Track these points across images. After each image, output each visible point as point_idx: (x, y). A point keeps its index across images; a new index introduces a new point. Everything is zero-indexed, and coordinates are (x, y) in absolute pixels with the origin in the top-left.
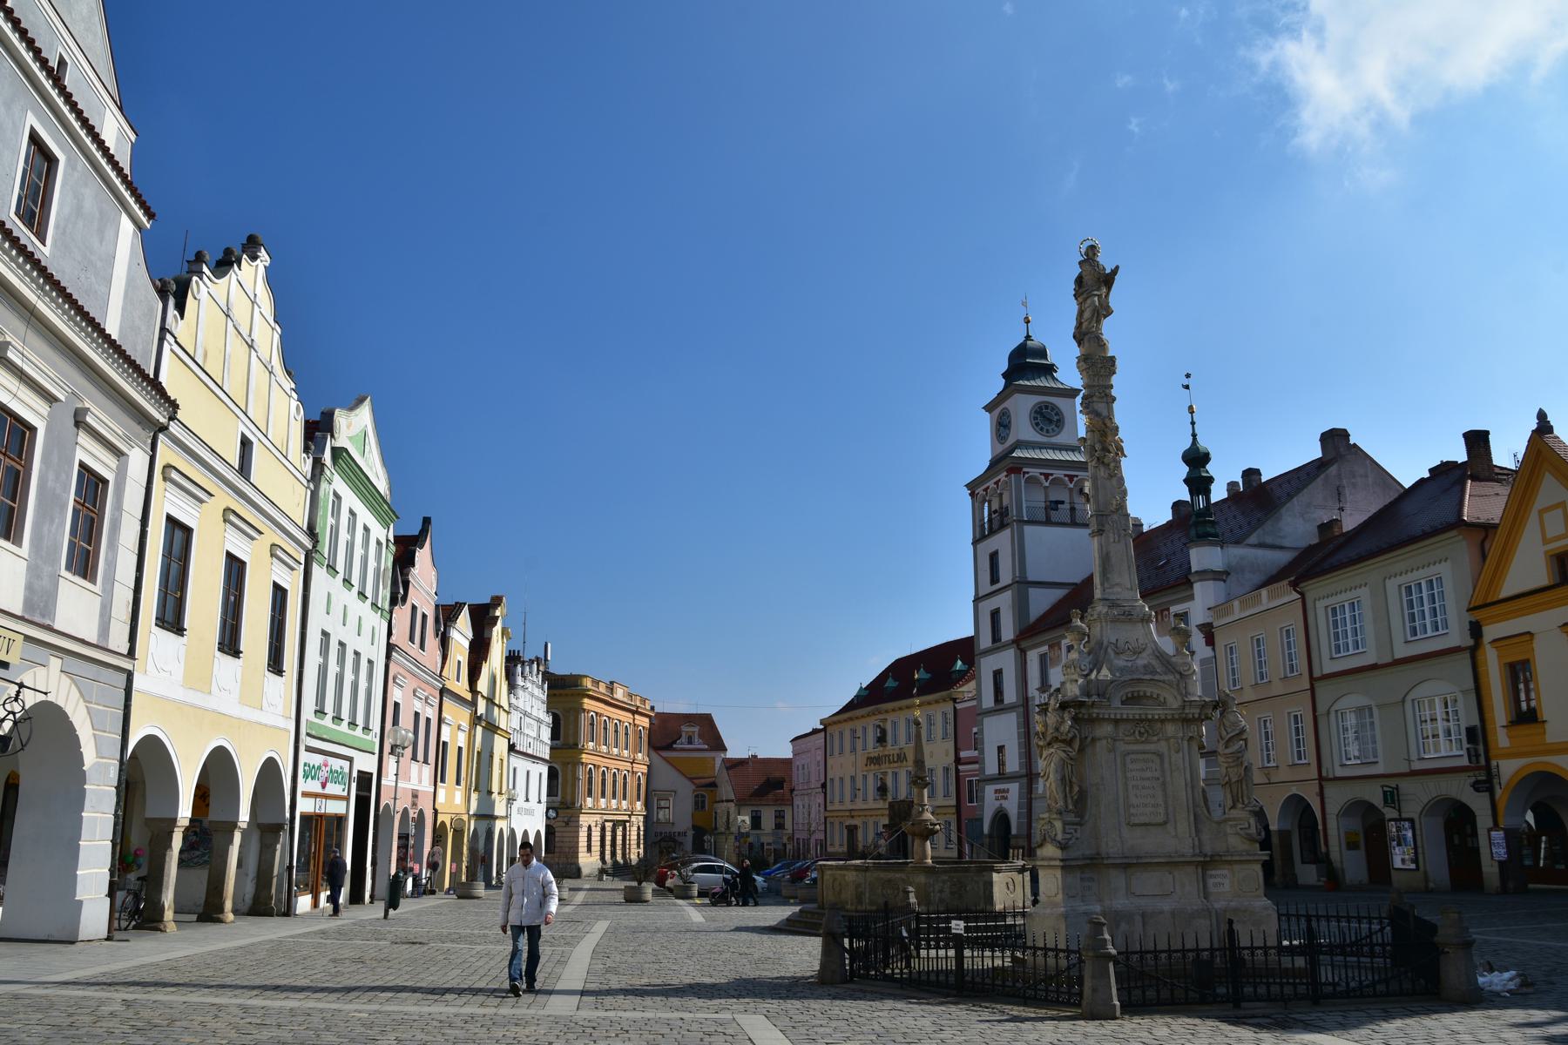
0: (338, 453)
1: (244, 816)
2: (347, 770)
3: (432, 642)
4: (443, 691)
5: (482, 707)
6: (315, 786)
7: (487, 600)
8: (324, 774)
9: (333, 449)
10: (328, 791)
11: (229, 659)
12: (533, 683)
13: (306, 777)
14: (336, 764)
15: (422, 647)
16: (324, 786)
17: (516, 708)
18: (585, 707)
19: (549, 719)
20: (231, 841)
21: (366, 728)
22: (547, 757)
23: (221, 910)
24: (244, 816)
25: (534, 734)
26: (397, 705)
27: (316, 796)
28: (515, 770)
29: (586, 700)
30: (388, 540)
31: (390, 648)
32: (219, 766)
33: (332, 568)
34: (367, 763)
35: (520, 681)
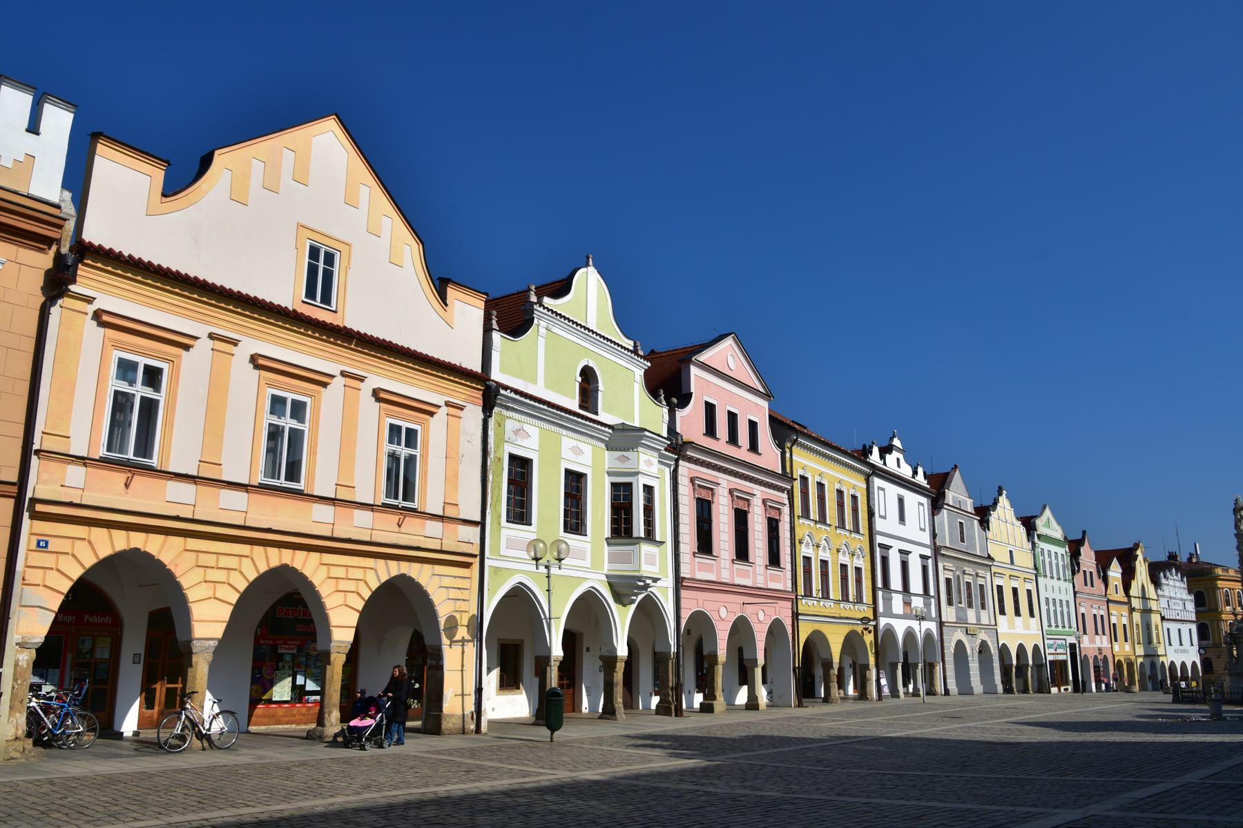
0: (1039, 536)
1: (1031, 662)
2: (1064, 643)
3: (1098, 583)
4: (1108, 601)
5: (1136, 603)
6: (1052, 651)
7: (1132, 546)
8: (1055, 646)
9: (1038, 535)
10: (1058, 651)
11: (1018, 617)
12: (1174, 580)
13: (1048, 648)
14: (1059, 642)
15: (1092, 586)
16: (1056, 650)
17: (1164, 596)
18: (1219, 586)
19: (1192, 597)
20: (1028, 670)
21: (1070, 627)
22: (1194, 619)
23: (1029, 690)
24: (1031, 662)
25: (1181, 608)
26: (1083, 614)
27: (1053, 654)
28: (1168, 629)
29: (1219, 582)
30: (1066, 552)
31: (1075, 593)
32: (1021, 648)
33: (1045, 576)
34: (1072, 640)
35: (1163, 581)
